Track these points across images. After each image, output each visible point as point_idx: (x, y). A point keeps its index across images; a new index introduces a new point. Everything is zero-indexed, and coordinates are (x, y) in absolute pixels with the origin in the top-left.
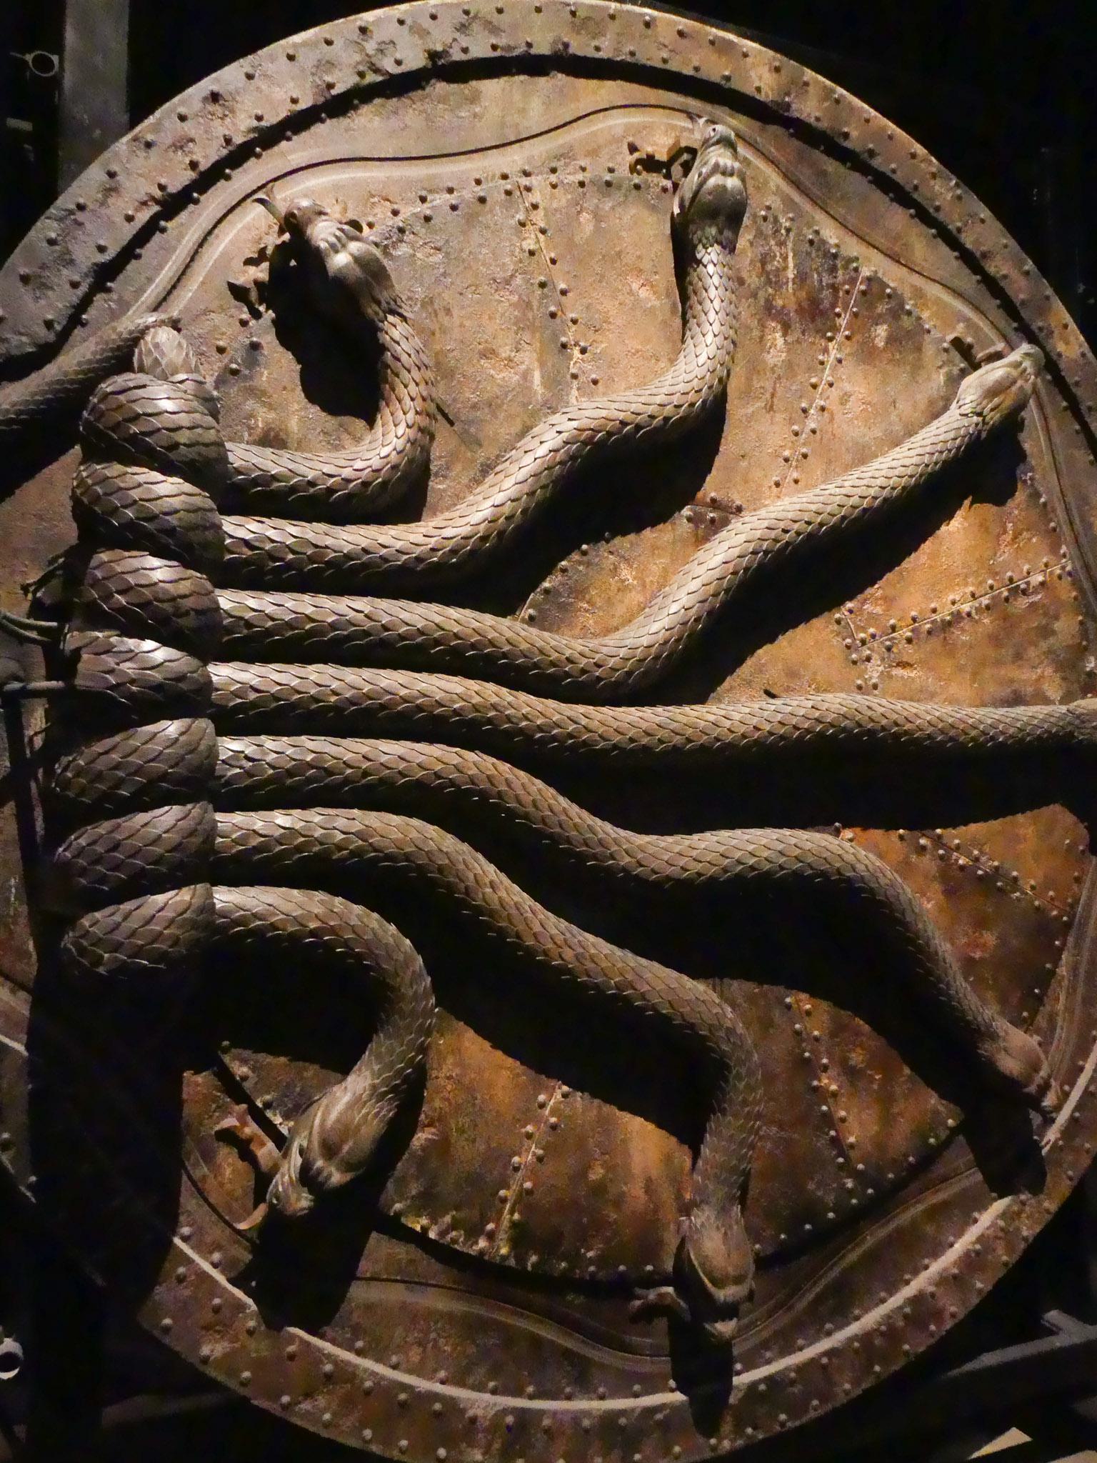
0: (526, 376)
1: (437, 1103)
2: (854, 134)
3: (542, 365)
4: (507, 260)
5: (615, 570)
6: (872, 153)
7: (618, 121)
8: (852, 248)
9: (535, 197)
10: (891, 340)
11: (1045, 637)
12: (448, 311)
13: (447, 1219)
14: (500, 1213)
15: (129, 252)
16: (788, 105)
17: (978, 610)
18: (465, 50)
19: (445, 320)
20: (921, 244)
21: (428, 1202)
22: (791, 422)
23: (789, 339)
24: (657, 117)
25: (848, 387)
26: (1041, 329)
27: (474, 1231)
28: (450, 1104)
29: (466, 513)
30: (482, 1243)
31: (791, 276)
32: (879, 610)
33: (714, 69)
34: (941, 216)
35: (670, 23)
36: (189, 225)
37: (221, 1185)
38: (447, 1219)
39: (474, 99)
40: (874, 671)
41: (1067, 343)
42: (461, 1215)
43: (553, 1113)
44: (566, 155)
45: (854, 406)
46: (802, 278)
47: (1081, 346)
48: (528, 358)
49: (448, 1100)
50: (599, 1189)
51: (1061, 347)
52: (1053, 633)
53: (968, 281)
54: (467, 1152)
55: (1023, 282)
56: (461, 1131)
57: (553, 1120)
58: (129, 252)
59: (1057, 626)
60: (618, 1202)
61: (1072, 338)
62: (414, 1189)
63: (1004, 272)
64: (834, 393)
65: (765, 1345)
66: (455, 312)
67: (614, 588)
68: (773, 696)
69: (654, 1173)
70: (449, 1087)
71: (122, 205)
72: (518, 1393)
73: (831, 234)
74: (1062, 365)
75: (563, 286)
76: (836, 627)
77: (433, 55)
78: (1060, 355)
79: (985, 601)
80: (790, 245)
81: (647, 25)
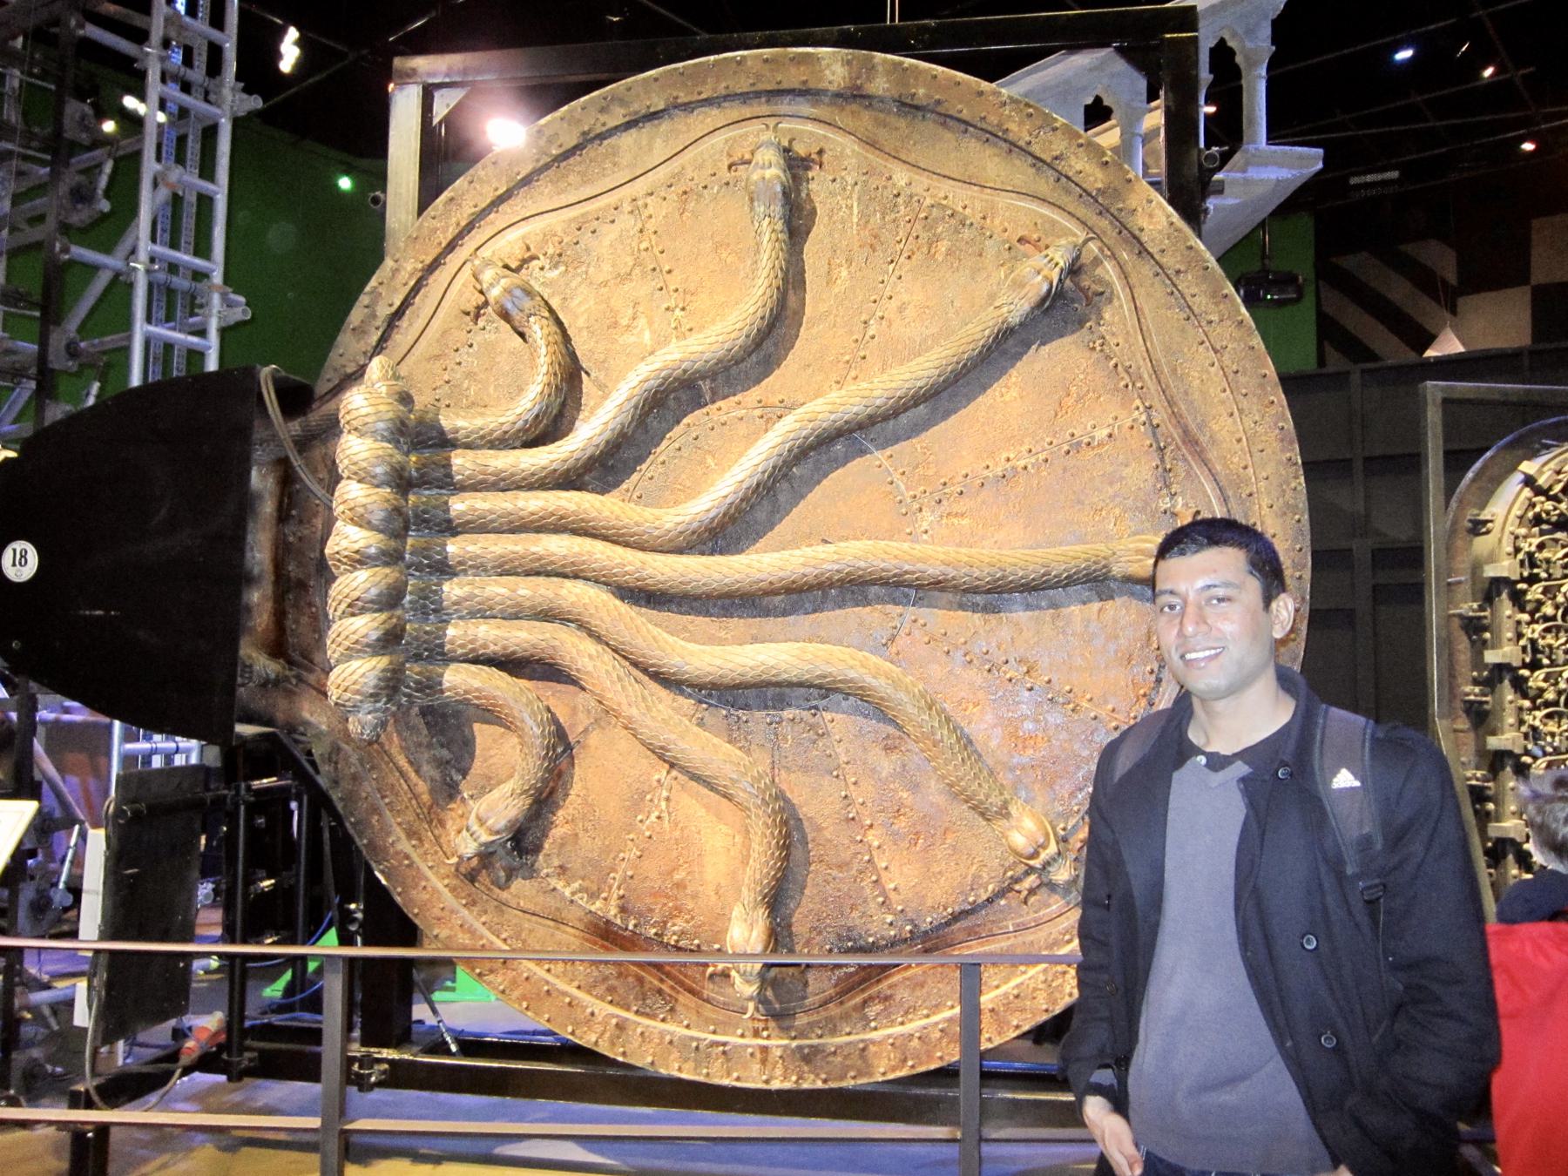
1: (571, 811)
2: (921, 91)
3: (650, 323)
5: (702, 462)
6: (938, 102)
7: (718, 139)
8: (923, 181)
9: (650, 210)
10: (949, 253)
11: (1111, 484)
13: (576, 885)
14: (610, 887)
15: (406, 303)
16: (859, 88)
17: (1036, 465)
18: (604, 124)
20: (992, 164)
21: (562, 870)
22: (851, 333)
23: (852, 269)
24: (756, 126)
25: (905, 298)
26: (1121, 210)
27: (593, 896)
29: (591, 429)
30: (598, 904)
31: (855, 220)
32: (931, 472)
33: (793, 77)
34: (1011, 137)
35: (756, 57)
36: (441, 277)
38: (576, 885)
39: (615, 152)
40: (927, 519)
41: (1151, 216)
42: (586, 883)
44: (678, 176)
45: (910, 312)
46: (865, 218)
47: (1168, 216)
50: (680, 885)
51: (1142, 221)
52: (1122, 478)
53: (1044, 185)
54: (589, 845)
55: (1099, 174)
58: (406, 303)
59: (1127, 472)
60: (695, 896)
61: (1158, 212)
62: (556, 863)
63: (1078, 167)
64: (894, 304)
65: (811, 1025)
68: (825, 542)
69: (723, 883)
71: (403, 275)
72: (628, 1009)
73: (901, 176)
74: (1144, 239)
75: (667, 268)
76: (889, 488)
77: (584, 133)
78: (1142, 230)
79: (1042, 457)
80: (855, 196)
81: (739, 63)
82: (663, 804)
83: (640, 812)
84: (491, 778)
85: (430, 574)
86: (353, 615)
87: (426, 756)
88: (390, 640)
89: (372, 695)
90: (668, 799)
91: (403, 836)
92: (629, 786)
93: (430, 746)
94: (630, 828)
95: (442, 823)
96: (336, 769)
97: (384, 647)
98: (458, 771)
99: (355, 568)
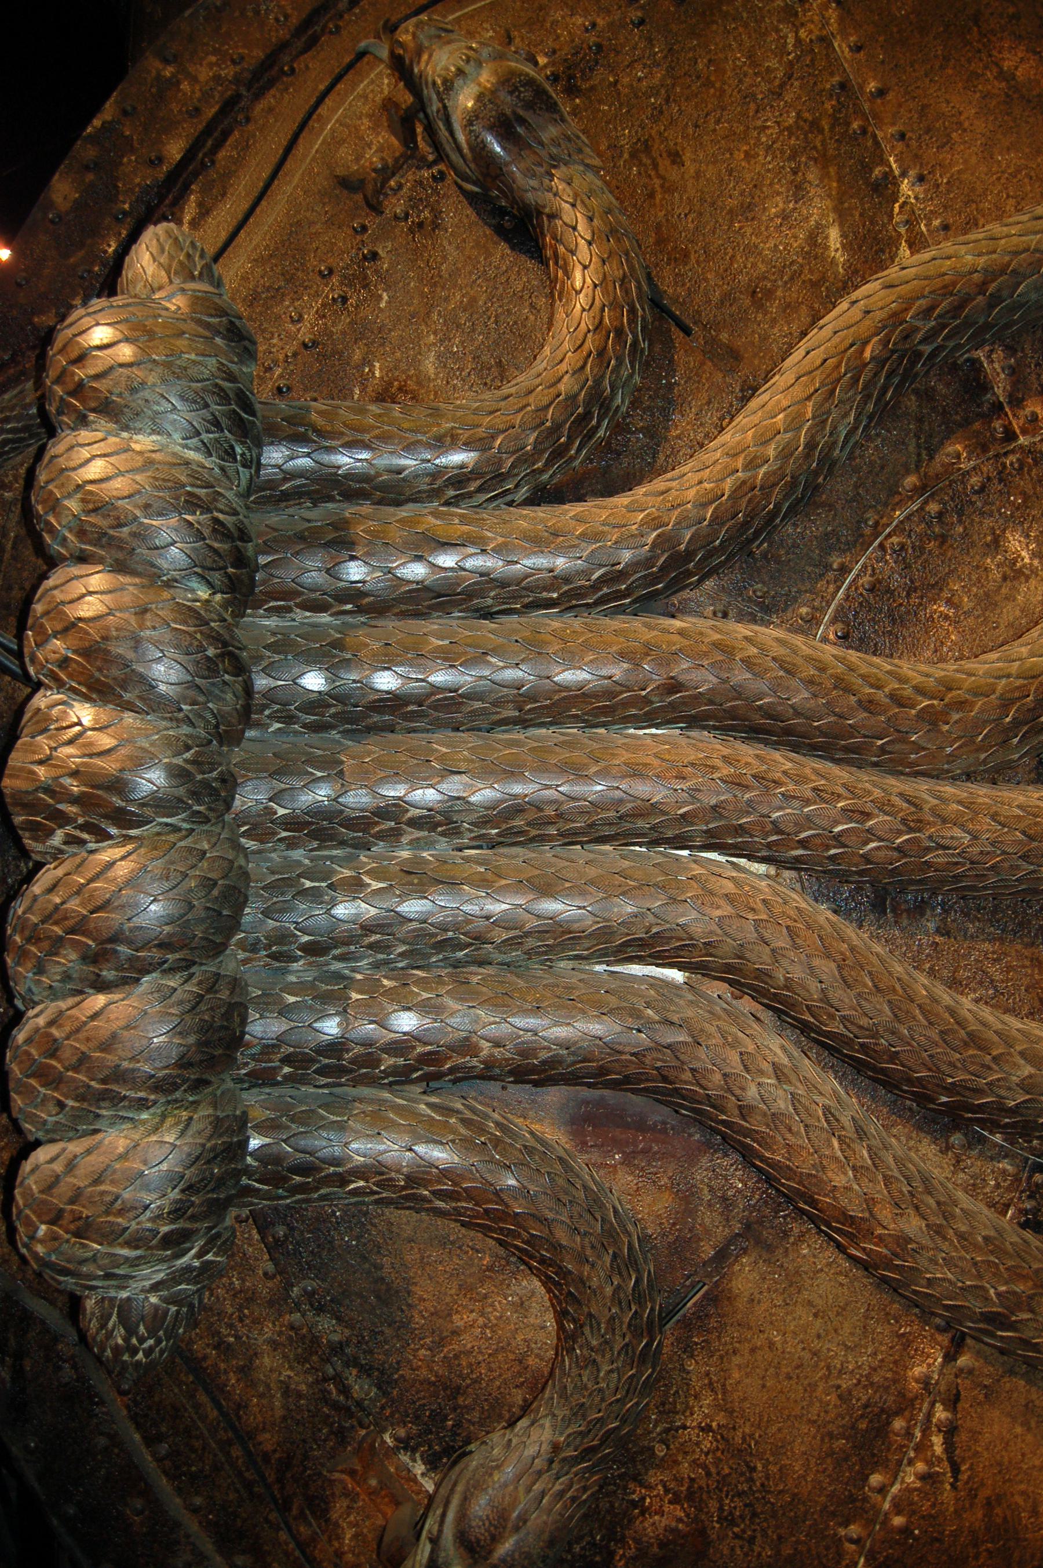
0: (815, 239)
1: (685, 1468)
3: (842, 216)
4: (773, 63)
12: (676, 158)
19: (673, 174)
28: (708, 1474)
37: (339, 1554)
43: (898, 1508)
48: (818, 207)
49: (705, 1467)
56: (728, 1520)
57: (898, 1521)
66: (687, 156)
67: (996, 575)
70: (706, 1445)
82: (937, 1442)
83: (876, 1463)
84: (458, 1391)
85: (291, 844)
86: (102, 986)
87: (269, 1330)
88: (214, 1047)
89: (167, 1241)
90: (950, 1431)
91: (208, 1546)
92: (845, 1397)
93: (279, 1302)
94: (853, 1505)
95: (318, 1506)
96: (18, 1372)
97: (199, 1084)
98: (366, 1371)
99: (103, 836)
